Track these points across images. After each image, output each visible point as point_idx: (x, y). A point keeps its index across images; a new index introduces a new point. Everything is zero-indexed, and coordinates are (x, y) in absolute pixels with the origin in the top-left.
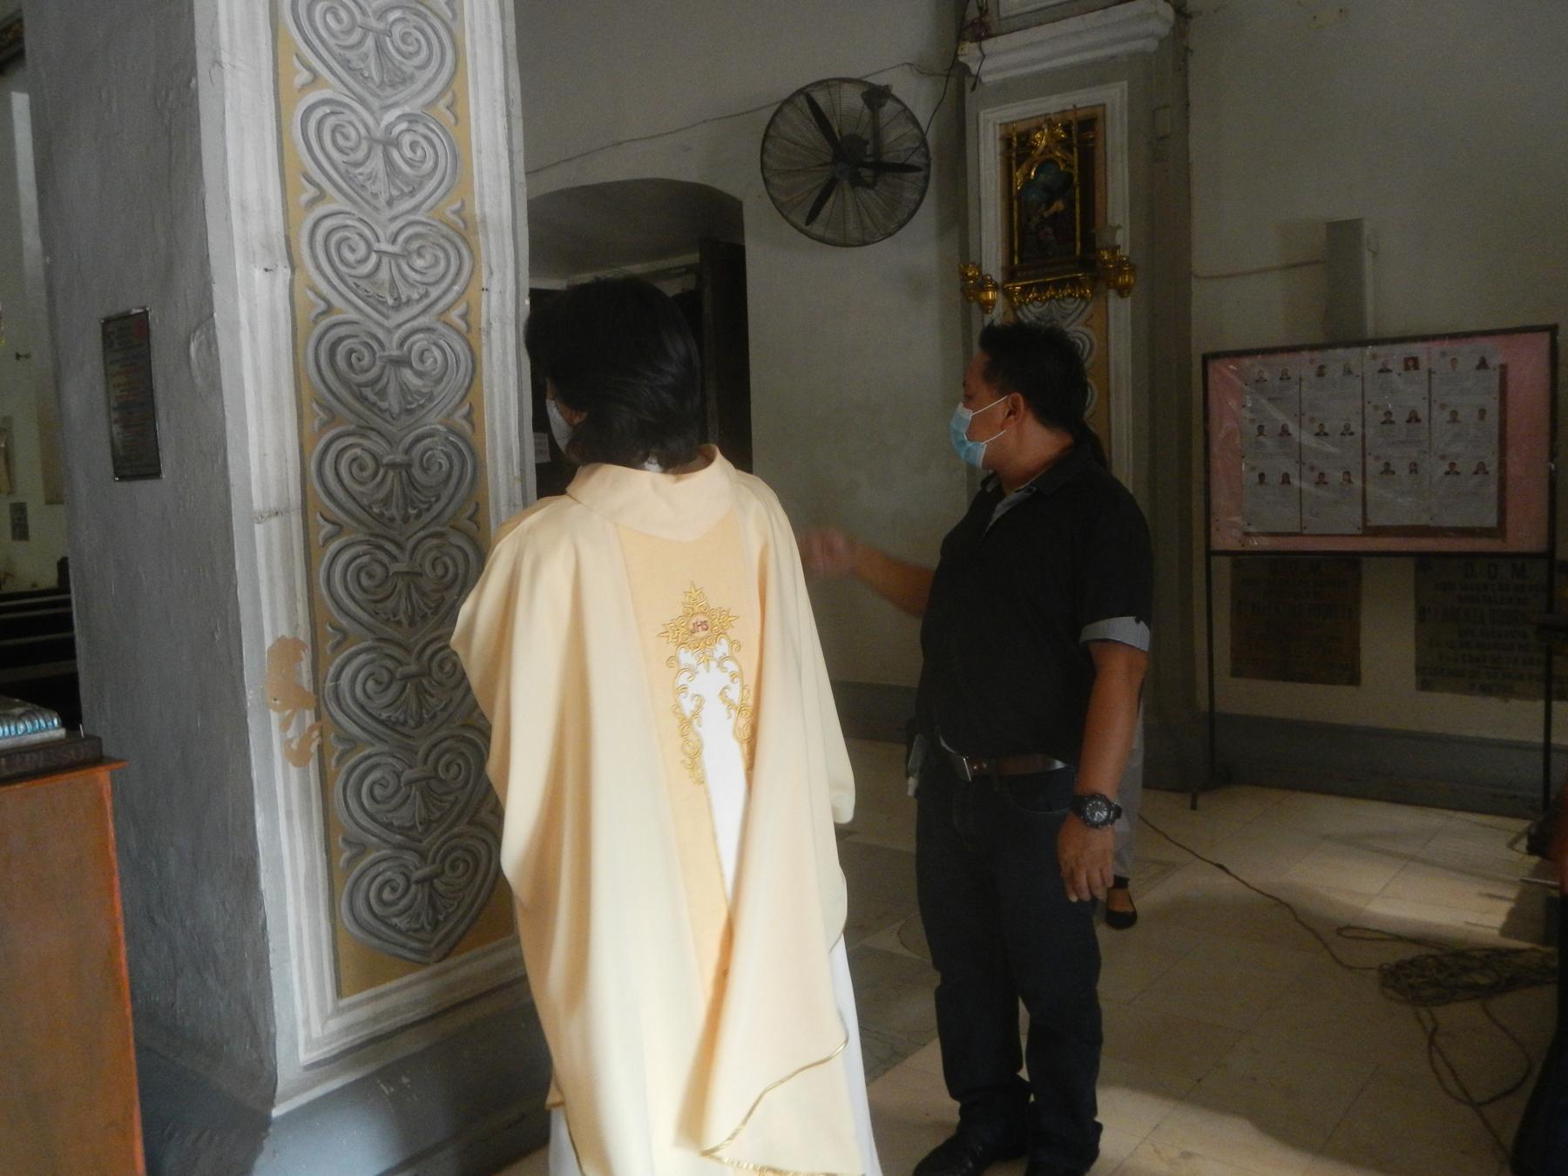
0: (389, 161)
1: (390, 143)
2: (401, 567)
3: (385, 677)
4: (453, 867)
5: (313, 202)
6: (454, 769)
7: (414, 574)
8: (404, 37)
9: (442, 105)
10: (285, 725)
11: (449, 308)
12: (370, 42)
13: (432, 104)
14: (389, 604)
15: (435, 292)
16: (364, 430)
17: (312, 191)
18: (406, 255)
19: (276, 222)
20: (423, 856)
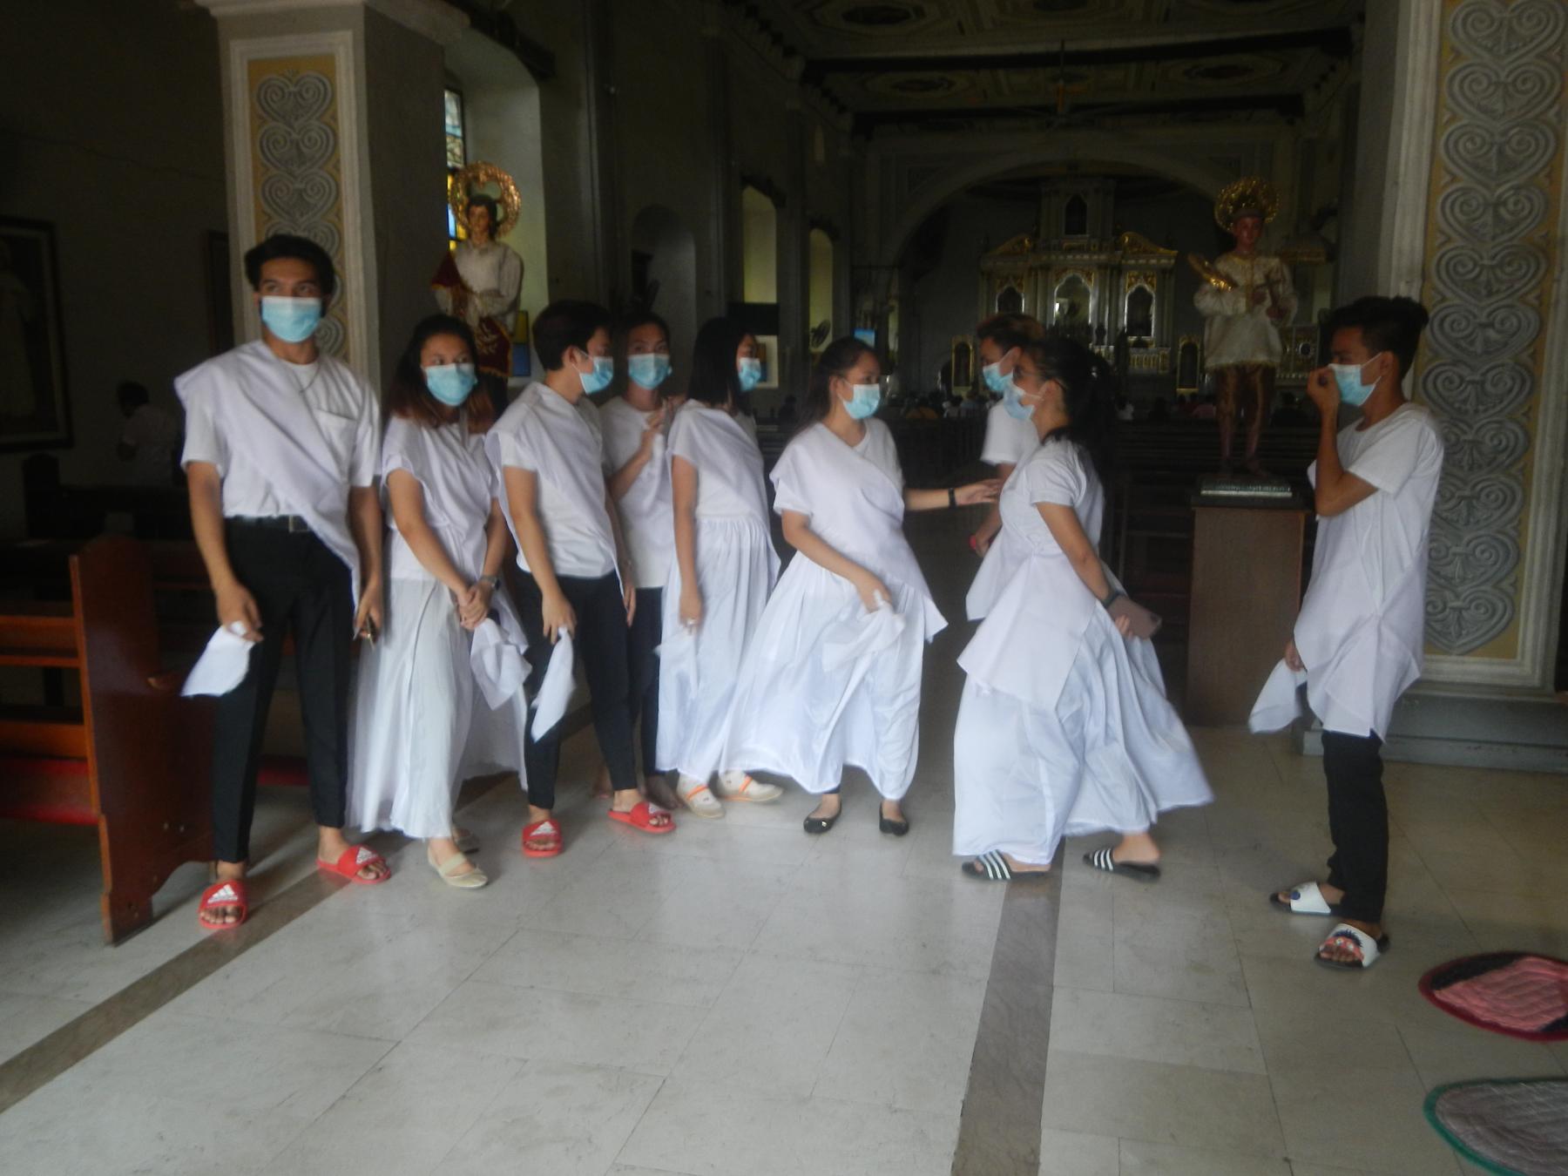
0: (1497, 216)
1: (1501, 203)
2: (1470, 437)
4: (1477, 608)
5: (1443, 244)
6: (1487, 555)
7: (1476, 444)
8: (1519, 143)
9: (1542, 175)
11: (1527, 294)
12: (1495, 150)
13: (1537, 174)
14: (1458, 456)
15: (1517, 286)
16: (1455, 363)
17: (1442, 239)
18: (1501, 265)
20: (1457, 596)
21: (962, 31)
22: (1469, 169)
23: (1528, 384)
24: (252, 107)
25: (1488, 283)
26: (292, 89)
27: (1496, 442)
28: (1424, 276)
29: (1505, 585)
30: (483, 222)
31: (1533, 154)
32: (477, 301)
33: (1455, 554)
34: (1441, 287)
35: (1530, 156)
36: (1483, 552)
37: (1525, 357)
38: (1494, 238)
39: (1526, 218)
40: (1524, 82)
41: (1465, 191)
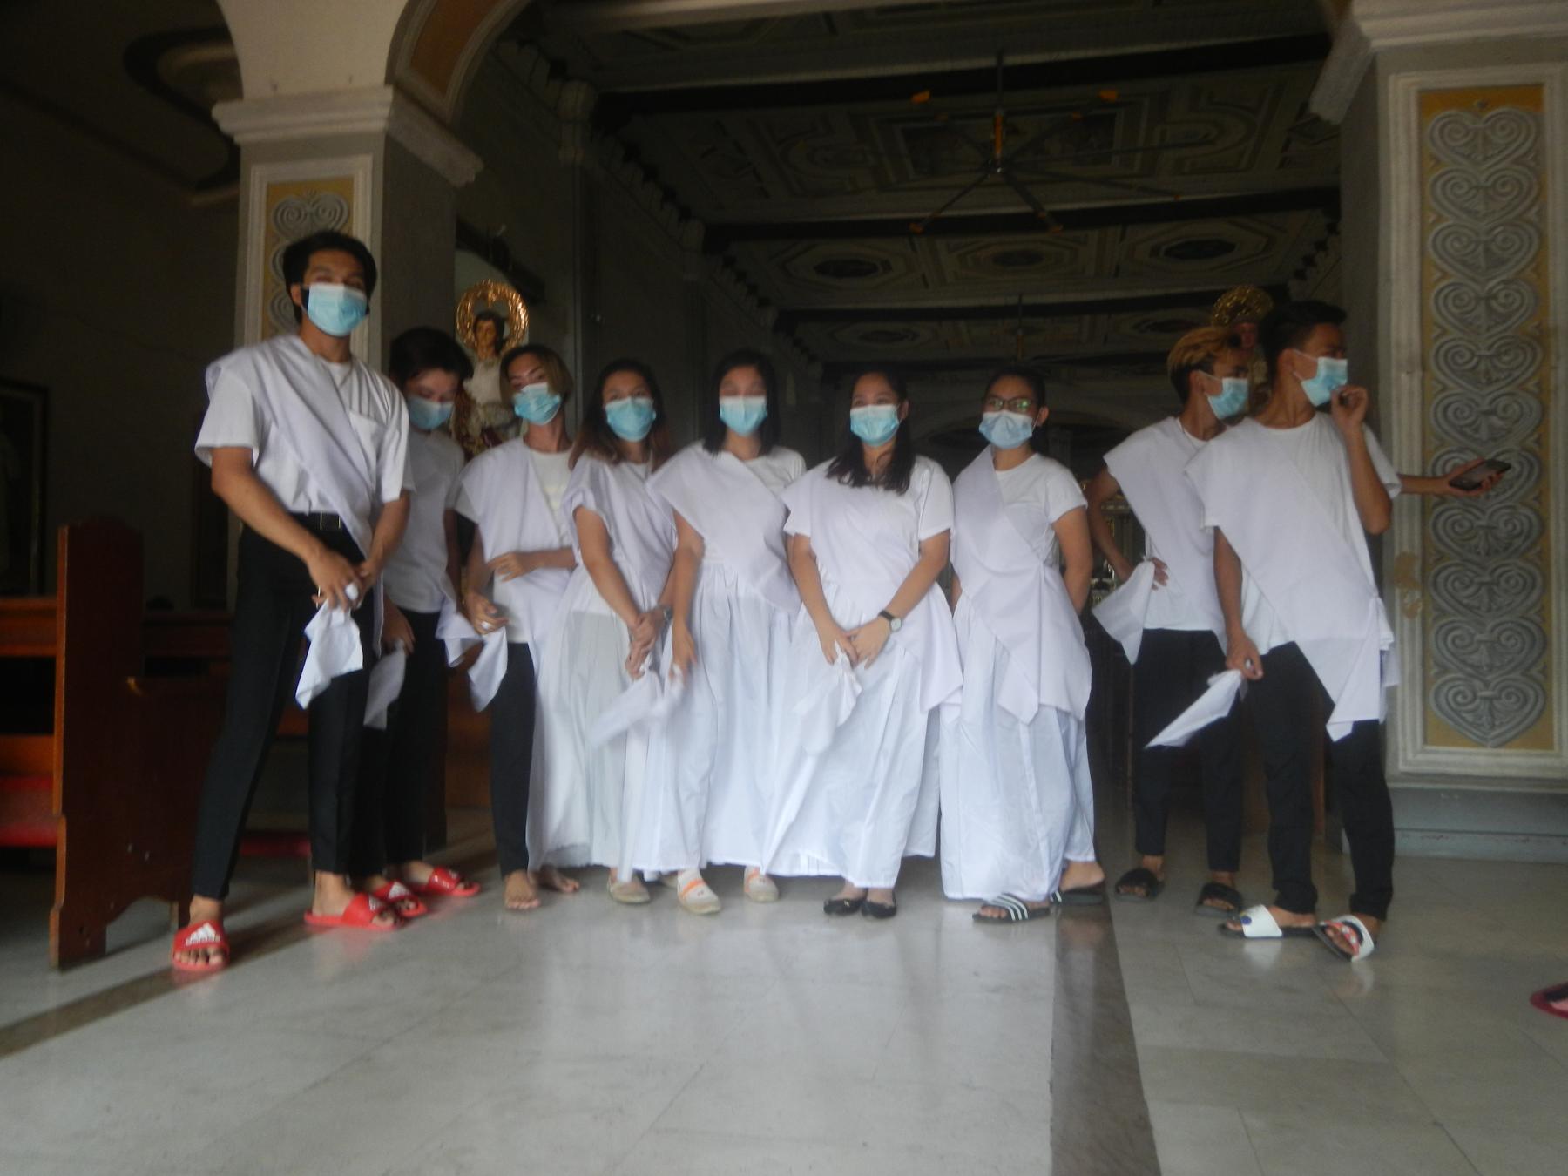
0: (1490, 310)
2: (1483, 523)
3: (1467, 580)
4: (1508, 696)
5: (1438, 337)
6: (1512, 641)
7: (1490, 529)
8: (1504, 240)
10: (1403, 596)
12: (1481, 248)
14: (1473, 542)
15: (1516, 373)
17: (1438, 331)
18: (1498, 355)
19: (1416, 348)
20: (1487, 685)
21: (926, 285)
22: (1459, 267)
23: (1536, 470)
24: (268, 225)
25: (1487, 372)
26: (309, 209)
27: (1510, 527)
28: (1424, 368)
29: (1534, 672)
30: (490, 337)
31: (1520, 249)
32: (481, 412)
33: (1480, 642)
34: (1442, 378)
35: (1516, 252)
36: (1508, 639)
37: (1530, 442)
38: (1488, 329)
39: (1518, 309)
40: (1504, 184)
41: (1456, 286)
